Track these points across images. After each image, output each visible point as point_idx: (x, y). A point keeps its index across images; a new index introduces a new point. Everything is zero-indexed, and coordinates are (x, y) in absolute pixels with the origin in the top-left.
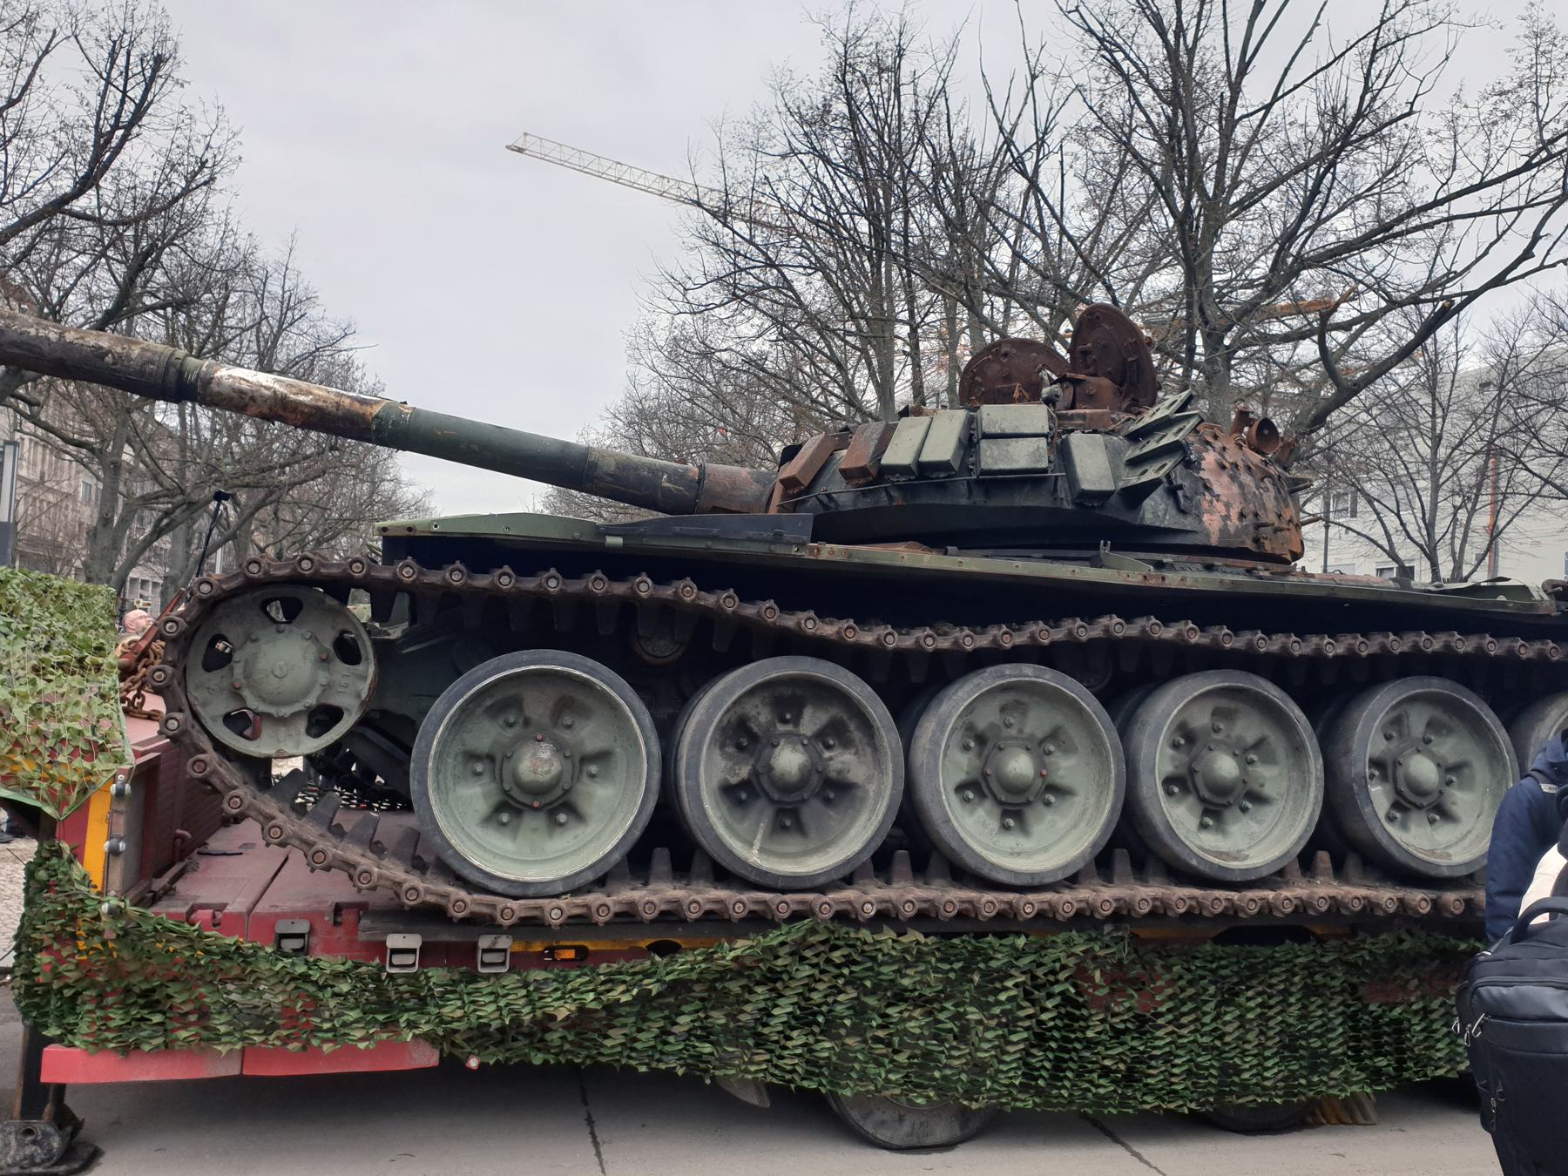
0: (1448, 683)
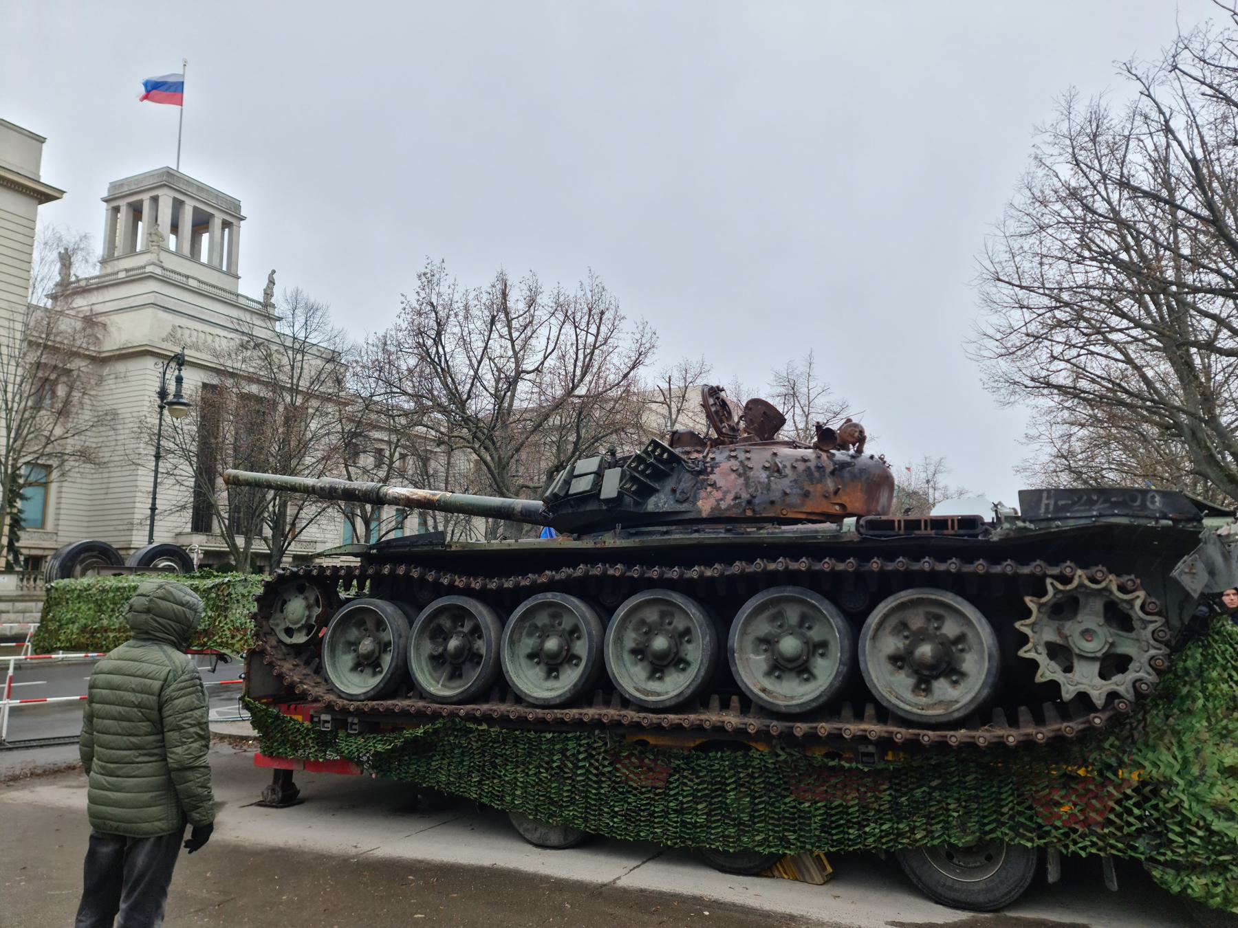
0: (798, 589)
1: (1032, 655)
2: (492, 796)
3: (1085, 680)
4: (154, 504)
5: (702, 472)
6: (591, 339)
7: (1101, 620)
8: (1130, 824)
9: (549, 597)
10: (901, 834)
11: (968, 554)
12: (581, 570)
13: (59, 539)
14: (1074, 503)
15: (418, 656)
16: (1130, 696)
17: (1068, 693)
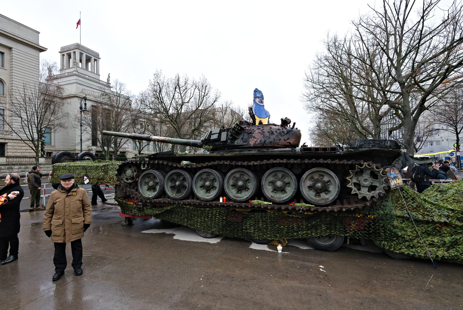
0: (282, 168)
1: (350, 186)
2: (191, 225)
3: (364, 192)
4: (81, 139)
5: (250, 133)
6: (203, 94)
7: (369, 176)
8: (371, 230)
9: (207, 170)
10: (308, 234)
11: (334, 157)
12: (216, 163)
14: (365, 143)
15: (167, 187)
16: (377, 197)
17: (360, 197)
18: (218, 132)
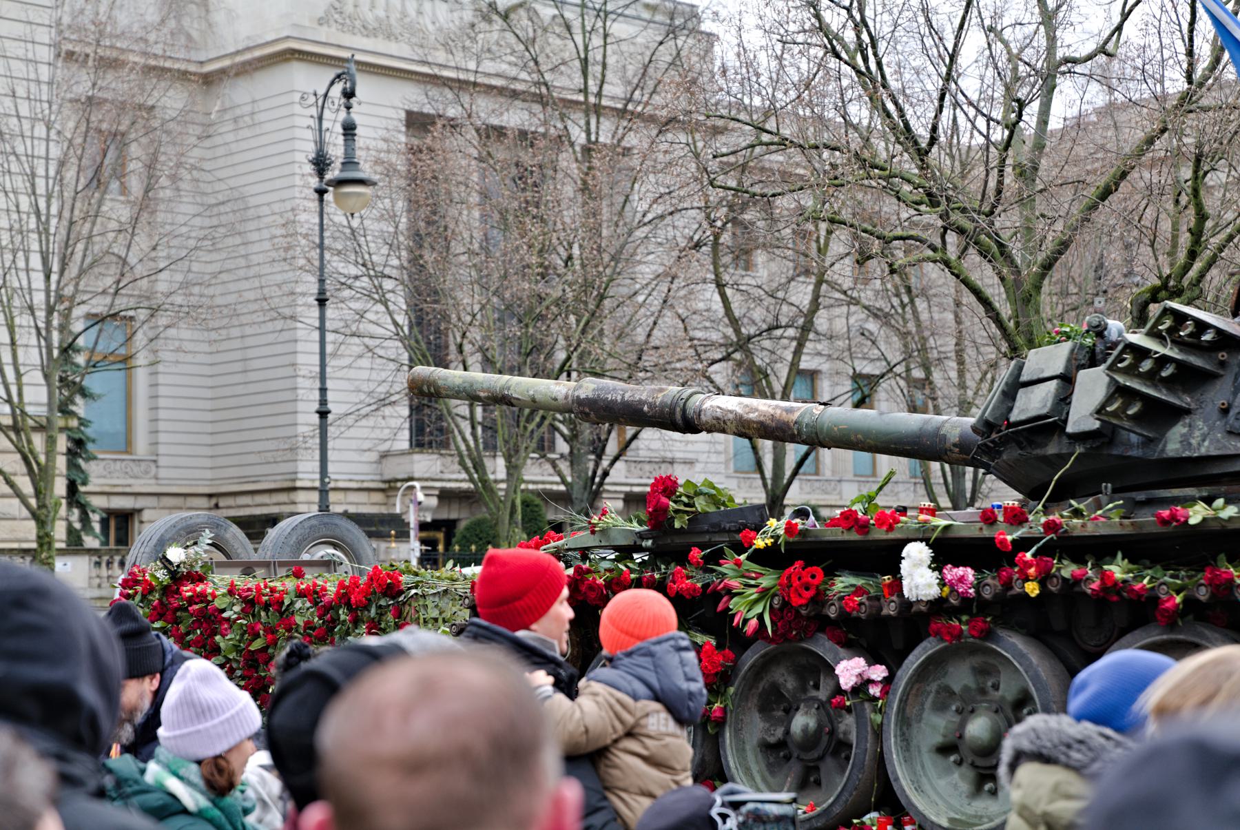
4: (323, 402)
13: (163, 473)
18: (1058, 367)
